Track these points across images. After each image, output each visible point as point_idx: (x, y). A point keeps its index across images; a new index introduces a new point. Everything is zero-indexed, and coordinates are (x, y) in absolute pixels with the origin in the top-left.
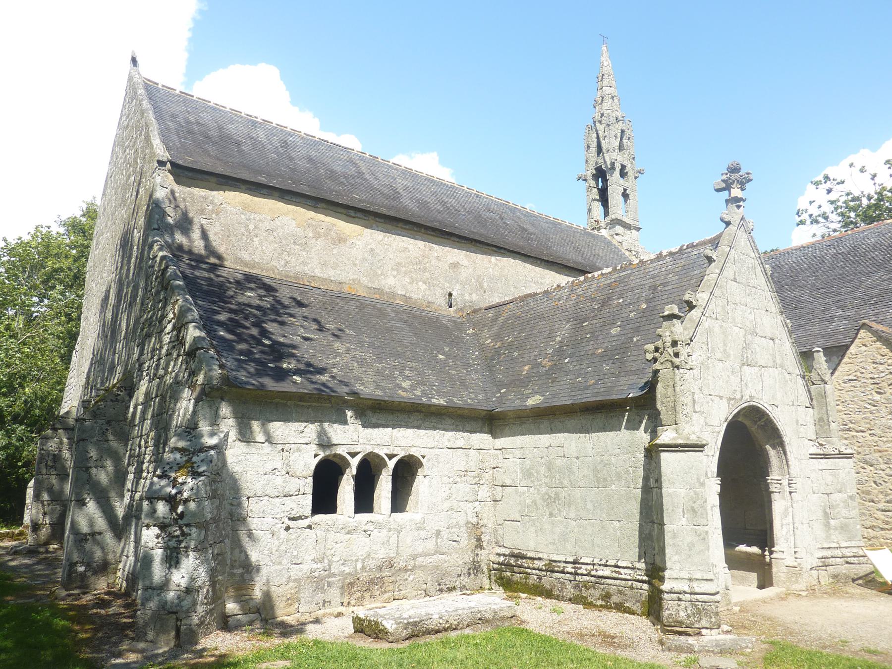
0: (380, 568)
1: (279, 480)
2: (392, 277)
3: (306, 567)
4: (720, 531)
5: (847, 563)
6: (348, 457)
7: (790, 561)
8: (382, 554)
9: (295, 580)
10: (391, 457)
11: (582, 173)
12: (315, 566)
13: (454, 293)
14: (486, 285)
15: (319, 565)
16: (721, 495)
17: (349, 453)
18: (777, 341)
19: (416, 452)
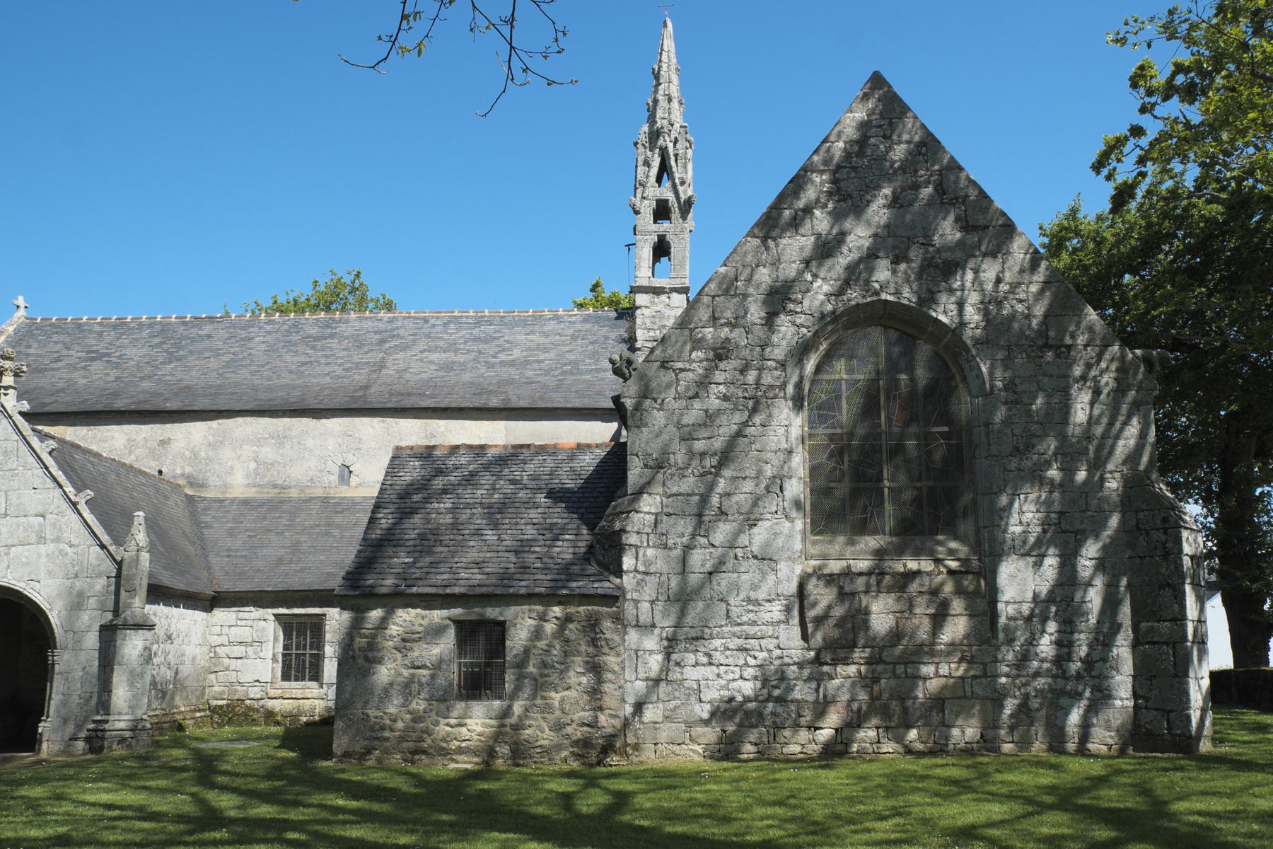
14: (203, 454)
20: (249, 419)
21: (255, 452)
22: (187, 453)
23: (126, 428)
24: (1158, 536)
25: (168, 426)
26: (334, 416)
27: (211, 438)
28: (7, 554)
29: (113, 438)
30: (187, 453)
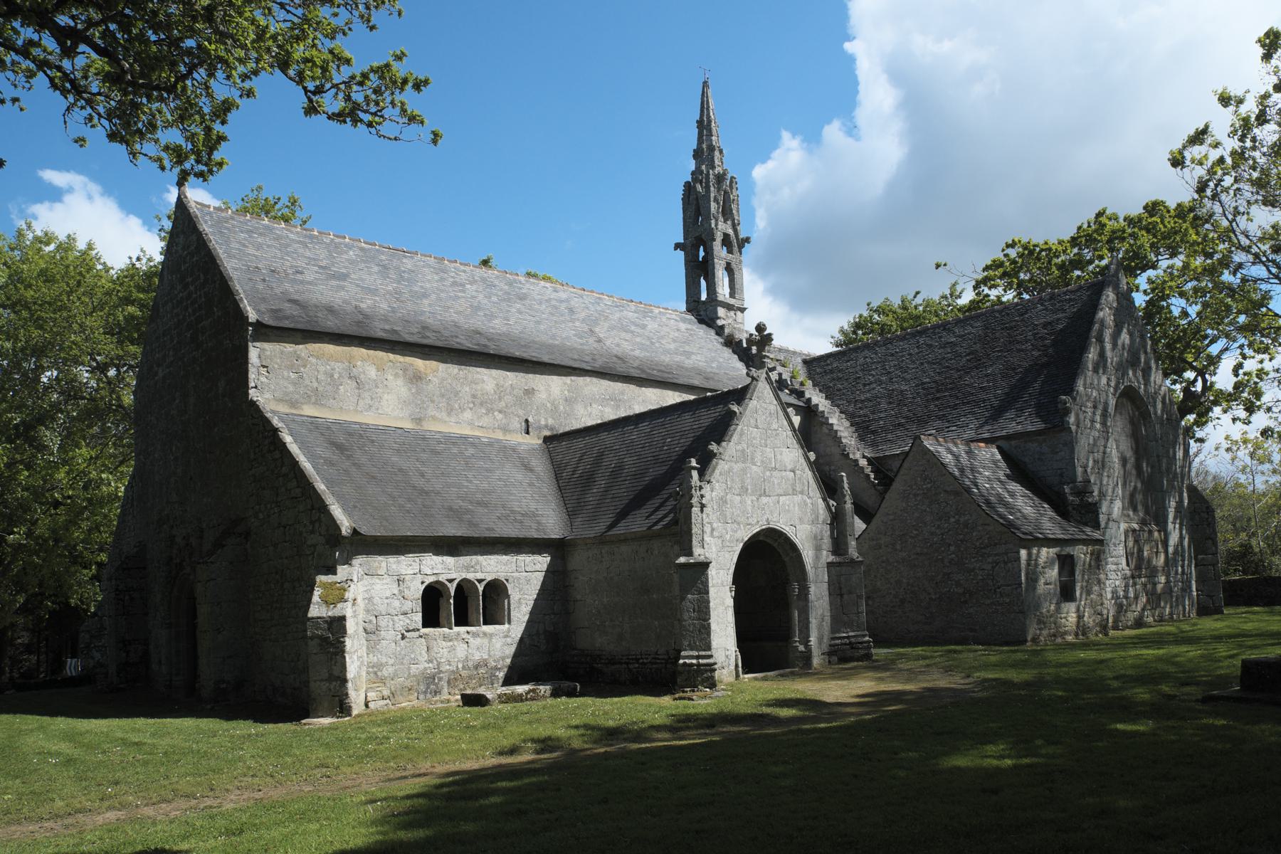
0: (476, 667)
1: (396, 603)
3: (421, 667)
5: (852, 648)
6: (447, 583)
7: (801, 648)
8: (477, 656)
9: (414, 676)
10: (480, 581)
12: (427, 665)
13: (530, 419)
14: (562, 407)
15: (431, 665)
16: (735, 599)
17: (447, 580)
18: (797, 472)
19: (502, 577)
20: (595, 380)
21: (601, 411)
22: (549, 405)
23: (494, 372)
25: (531, 376)
26: (651, 386)
27: (566, 392)
28: (778, 502)
30: (549, 405)
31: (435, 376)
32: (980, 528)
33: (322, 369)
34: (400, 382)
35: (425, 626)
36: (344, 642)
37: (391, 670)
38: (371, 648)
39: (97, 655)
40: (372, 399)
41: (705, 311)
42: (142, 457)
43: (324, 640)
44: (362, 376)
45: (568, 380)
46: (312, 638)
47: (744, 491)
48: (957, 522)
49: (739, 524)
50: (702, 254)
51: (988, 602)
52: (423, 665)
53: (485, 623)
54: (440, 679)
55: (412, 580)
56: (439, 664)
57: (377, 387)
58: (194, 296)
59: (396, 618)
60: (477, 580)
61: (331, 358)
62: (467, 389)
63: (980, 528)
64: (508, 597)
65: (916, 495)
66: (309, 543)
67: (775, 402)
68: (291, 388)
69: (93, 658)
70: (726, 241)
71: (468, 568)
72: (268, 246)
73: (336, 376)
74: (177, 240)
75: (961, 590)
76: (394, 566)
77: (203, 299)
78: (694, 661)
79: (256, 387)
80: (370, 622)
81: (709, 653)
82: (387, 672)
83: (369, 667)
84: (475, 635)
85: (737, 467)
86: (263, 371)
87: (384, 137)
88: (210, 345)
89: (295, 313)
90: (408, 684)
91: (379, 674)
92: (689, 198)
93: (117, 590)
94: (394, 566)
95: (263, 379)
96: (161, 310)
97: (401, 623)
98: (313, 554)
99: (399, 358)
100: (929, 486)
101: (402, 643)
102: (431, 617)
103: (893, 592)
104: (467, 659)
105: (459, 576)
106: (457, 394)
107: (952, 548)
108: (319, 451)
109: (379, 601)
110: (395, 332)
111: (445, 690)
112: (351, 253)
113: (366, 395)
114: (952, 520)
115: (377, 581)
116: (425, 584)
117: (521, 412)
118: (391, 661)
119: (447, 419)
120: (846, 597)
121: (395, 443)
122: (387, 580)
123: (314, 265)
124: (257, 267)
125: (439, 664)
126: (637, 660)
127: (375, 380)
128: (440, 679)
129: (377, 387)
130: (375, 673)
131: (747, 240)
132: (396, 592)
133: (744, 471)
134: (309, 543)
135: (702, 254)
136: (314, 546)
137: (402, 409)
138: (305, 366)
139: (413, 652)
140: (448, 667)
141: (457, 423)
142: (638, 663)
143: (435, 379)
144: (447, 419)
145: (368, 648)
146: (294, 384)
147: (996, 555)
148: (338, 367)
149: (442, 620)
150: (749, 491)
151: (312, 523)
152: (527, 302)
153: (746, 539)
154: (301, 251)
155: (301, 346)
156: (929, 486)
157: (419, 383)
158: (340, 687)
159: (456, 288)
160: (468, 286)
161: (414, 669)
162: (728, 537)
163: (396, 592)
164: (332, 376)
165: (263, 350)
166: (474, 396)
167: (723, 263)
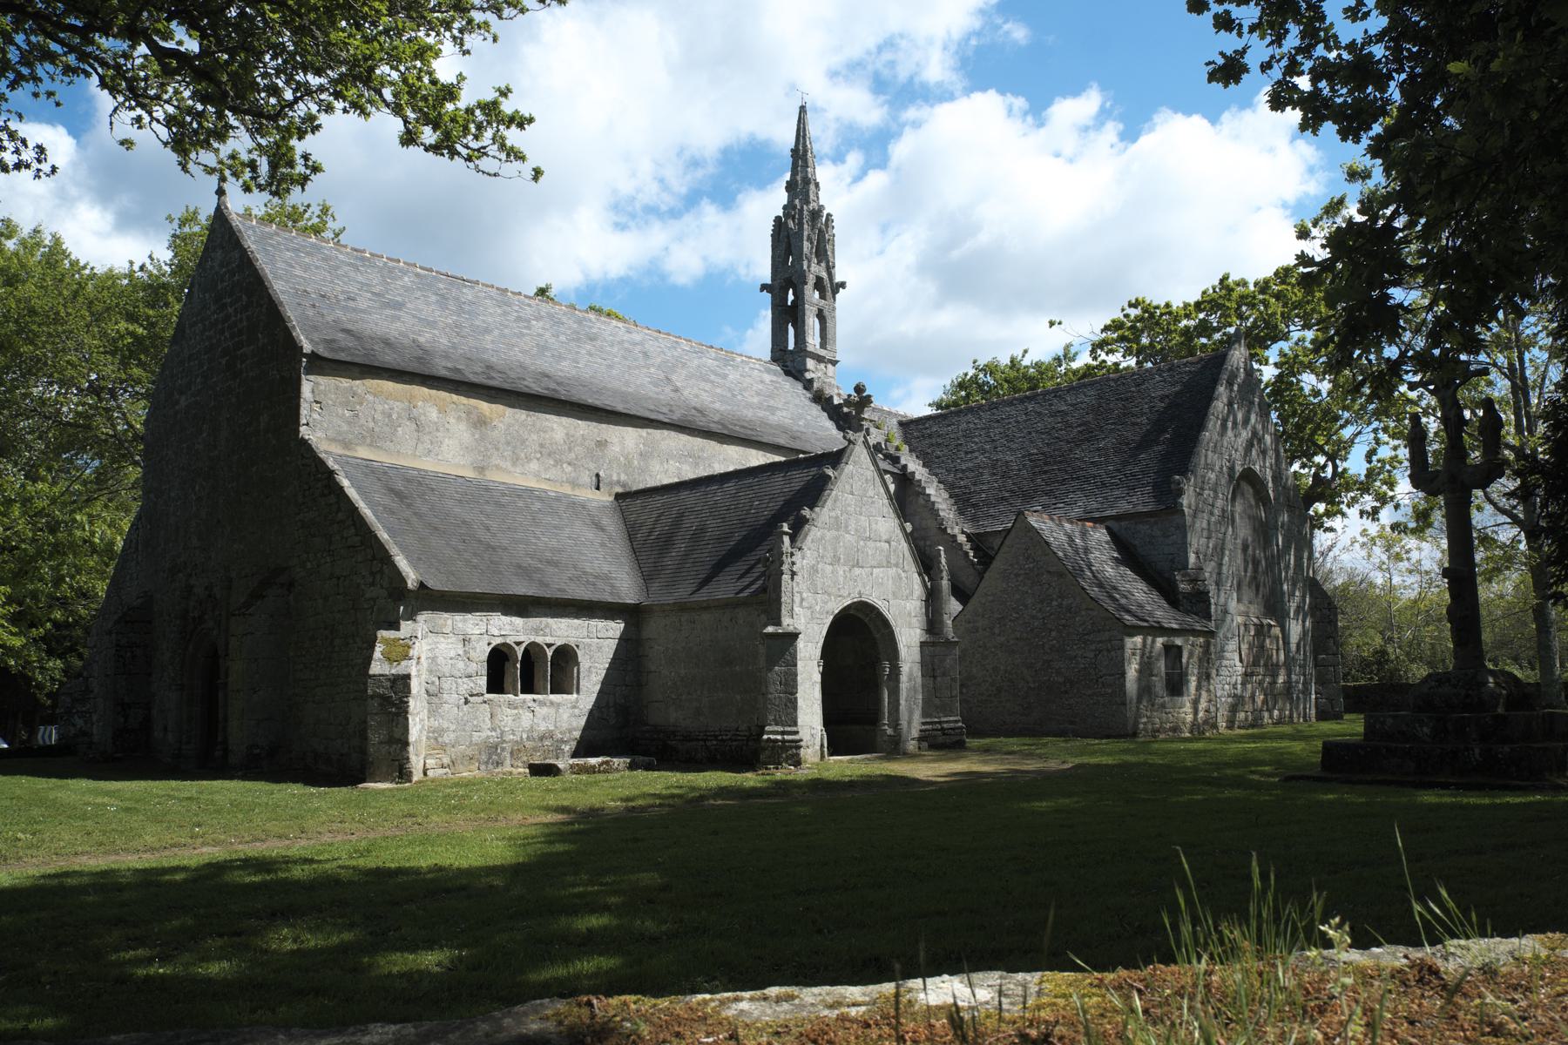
0: (542, 739)
1: (461, 665)
2: (535, 461)
3: (483, 735)
4: (820, 702)
5: (944, 734)
6: (514, 645)
7: (890, 731)
8: (543, 727)
10: (549, 645)
11: (769, 281)
12: (490, 734)
13: (602, 474)
14: (636, 462)
15: (494, 734)
16: (823, 675)
19: (572, 642)
21: (678, 468)
23: (565, 420)
24: (1326, 612)
25: (604, 426)
26: (732, 444)
27: (641, 446)
28: (872, 574)
29: (553, 430)
31: (501, 422)
32: (1083, 613)
33: (379, 408)
34: (463, 426)
35: (489, 691)
36: (408, 702)
37: (452, 736)
38: (433, 713)
39: (80, 722)
40: (432, 443)
41: (793, 361)
42: (152, 496)
43: (385, 699)
44: (423, 418)
45: (644, 432)
46: (372, 697)
47: (836, 560)
48: (1060, 606)
49: (829, 595)
50: (791, 297)
51: (1090, 692)
52: (486, 734)
53: (552, 693)
54: (503, 749)
55: (478, 641)
56: (502, 733)
57: (437, 430)
58: (233, 319)
59: (459, 680)
60: (546, 644)
61: (389, 396)
62: (535, 437)
63: (1083, 613)
64: (578, 664)
65: (1017, 575)
66: (368, 596)
67: (872, 468)
68: (345, 427)
69: (74, 725)
70: (819, 285)
71: (537, 631)
72: (317, 267)
73: (395, 416)
74: (212, 255)
75: (1061, 680)
76: (460, 625)
77: (245, 323)
78: (779, 737)
79: (307, 424)
80: (433, 683)
81: (794, 729)
82: (448, 738)
83: (428, 732)
84: (542, 704)
85: (829, 535)
86: (316, 407)
87: (483, 172)
88: (251, 374)
89: (350, 345)
90: (469, 752)
91: (440, 740)
92: (779, 234)
93: (118, 645)
94: (460, 625)
95: (316, 416)
96: (188, 331)
97: (465, 686)
98: (372, 608)
99: (463, 400)
100: (1031, 565)
101: (465, 708)
102: (496, 683)
103: (990, 680)
104: (532, 729)
105: (527, 639)
106: (523, 442)
107: (1054, 634)
108: (377, 497)
109: (444, 662)
110: (458, 371)
111: (508, 762)
112: (406, 279)
113: (426, 438)
114: (1055, 603)
115: (442, 639)
116: (492, 646)
117: (592, 466)
118: (453, 727)
119: (512, 469)
120: (939, 679)
121: (457, 492)
122: (453, 639)
123: (366, 291)
124: (305, 291)
125: (502, 733)
126: (716, 736)
127: (436, 423)
128: (503, 749)
129: (437, 430)
130: (436, 739)
131: (843, 285)
132: (461, 652)
133: (837, 538)
134: (368, 596)
135: (791, 297)
136: (374, 600)
137: (463, 456)
138: (361, 404)
139: (476, 718)
140: (511, 737)
141: (522, 474)
142: (717, 740)
143: (501, 425)
144: (512, 469)
145: (429, 711)
146: (349, 423)
147: (1100, 642)
148: (398, 406)
149: (507, 685)
150: (842, 561)
151: (373, 574)
152: (599, 343)
153: (836, 612)
154: (352, 274)
155: (358, 382)
156: (1031, 565)
157: (483, 429)
158: (401, 751)
159: (521, 324)
160: (534, 322)
161: (476, 737)
162: (818, 608)
163: (461, 652)
164: (390, 416)
165: (317, 384)
166: (542, 446)
167: (815, 309)
